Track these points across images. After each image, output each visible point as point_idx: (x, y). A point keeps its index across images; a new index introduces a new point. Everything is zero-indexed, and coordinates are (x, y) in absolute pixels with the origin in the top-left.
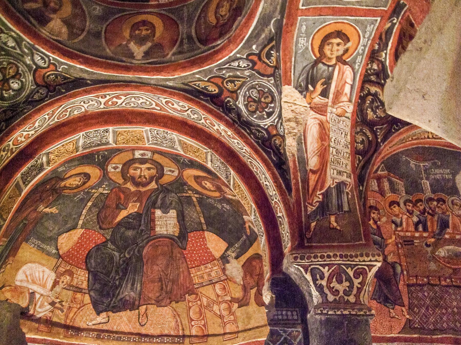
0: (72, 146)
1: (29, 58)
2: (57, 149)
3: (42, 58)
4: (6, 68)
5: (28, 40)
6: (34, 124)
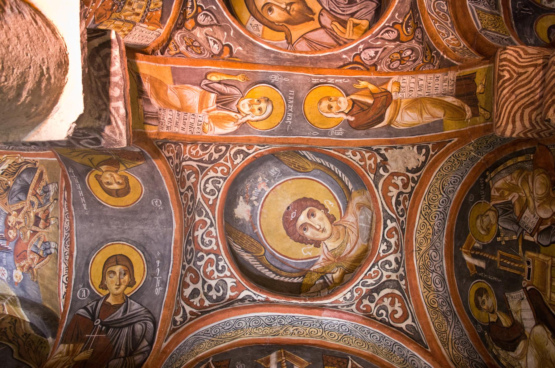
0: (487, 16)
1: (386, 43)
2: (482, 23)
3: (387, 32)
4: (392, 59)
5: (367, 37)
6: (439, 32)
